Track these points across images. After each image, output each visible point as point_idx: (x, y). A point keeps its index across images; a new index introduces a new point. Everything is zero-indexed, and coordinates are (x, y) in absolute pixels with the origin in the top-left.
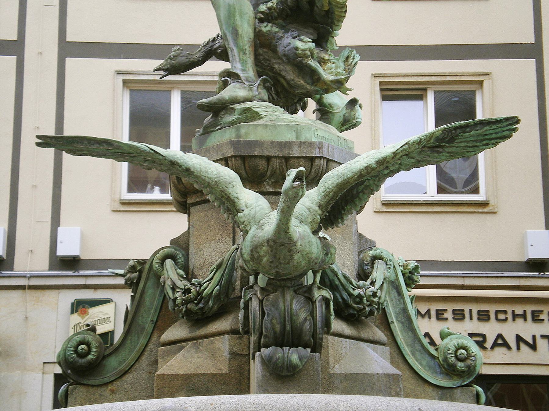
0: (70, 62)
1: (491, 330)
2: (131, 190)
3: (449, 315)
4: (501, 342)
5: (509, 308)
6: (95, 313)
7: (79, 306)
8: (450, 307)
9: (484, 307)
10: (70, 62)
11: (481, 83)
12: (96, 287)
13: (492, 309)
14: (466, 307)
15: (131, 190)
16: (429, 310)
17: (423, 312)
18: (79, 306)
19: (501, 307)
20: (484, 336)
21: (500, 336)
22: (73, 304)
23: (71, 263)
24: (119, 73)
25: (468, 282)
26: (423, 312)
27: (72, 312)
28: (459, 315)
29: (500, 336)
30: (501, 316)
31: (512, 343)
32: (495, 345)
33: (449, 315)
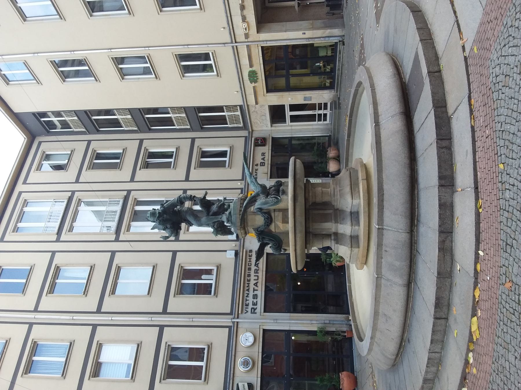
3: (249, 278)
5: (248, 263)
8: (247, 278)
9: (247, 269)
13: (247, 267)
14: (247, 273)
17: (247, 285)
19: (247, 264)
25: (240, 272)
28: (249, 275)
32: (257, 267)
33: (249, 278)
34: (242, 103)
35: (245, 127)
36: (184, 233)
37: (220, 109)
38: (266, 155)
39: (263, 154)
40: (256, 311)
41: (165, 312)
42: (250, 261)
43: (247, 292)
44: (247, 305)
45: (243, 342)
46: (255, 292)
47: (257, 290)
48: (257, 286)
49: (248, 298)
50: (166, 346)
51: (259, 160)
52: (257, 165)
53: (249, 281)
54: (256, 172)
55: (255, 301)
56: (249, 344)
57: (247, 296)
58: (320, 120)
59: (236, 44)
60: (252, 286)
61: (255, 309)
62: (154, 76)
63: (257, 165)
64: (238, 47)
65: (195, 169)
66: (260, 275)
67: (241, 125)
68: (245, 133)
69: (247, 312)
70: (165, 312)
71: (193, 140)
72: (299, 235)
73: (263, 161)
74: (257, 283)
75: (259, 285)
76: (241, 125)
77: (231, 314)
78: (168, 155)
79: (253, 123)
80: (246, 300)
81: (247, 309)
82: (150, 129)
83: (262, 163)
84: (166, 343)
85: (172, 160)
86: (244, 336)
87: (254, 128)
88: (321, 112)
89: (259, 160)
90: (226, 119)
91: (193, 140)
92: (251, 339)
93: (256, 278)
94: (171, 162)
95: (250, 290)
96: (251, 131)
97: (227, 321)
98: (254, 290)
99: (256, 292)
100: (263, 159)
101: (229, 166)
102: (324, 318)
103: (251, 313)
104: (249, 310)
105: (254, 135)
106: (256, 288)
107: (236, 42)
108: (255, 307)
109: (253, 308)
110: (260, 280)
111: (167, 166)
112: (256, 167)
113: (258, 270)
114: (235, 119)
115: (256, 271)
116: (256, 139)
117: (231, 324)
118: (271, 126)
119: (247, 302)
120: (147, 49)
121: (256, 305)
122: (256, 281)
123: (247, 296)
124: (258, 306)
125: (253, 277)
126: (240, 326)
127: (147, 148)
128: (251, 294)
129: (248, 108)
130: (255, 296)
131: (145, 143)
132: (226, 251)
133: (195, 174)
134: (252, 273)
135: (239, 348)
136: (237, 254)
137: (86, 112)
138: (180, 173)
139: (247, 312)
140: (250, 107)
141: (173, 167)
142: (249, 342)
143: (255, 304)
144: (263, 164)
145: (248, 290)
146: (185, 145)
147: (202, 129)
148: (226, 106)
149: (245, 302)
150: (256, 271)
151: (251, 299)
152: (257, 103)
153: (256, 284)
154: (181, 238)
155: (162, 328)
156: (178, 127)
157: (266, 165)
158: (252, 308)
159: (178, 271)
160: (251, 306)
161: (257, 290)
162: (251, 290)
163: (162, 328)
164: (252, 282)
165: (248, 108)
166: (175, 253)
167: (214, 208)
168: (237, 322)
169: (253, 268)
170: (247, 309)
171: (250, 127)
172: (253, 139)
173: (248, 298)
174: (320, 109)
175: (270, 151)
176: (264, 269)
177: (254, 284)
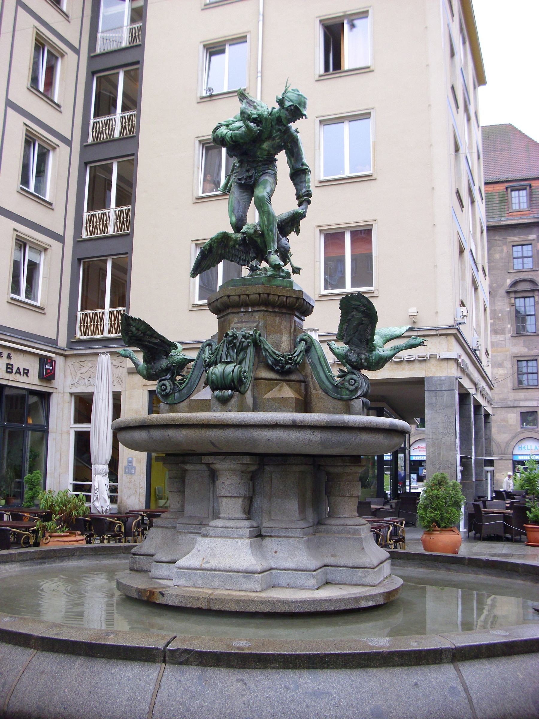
35: (73, 343)
58: (76, 488)
62: (201, 194)
67: (78, 336)
68: (63, 342)
72: (317, 436)
76: (78, 336)
79: (83, 359)
82: (86, 164)
87: (70, 361)
90: (97, 308)
91: (60, 239)
96: (67, 353)
105: (58, 357)
116: (52, 362)
118: (71, 394)
127: (58, 149)
131: (63, 148)
137: (138, 63)
146: (53, 220)
147: (78, 260)
171: (75, 352)
172: (53, 355)
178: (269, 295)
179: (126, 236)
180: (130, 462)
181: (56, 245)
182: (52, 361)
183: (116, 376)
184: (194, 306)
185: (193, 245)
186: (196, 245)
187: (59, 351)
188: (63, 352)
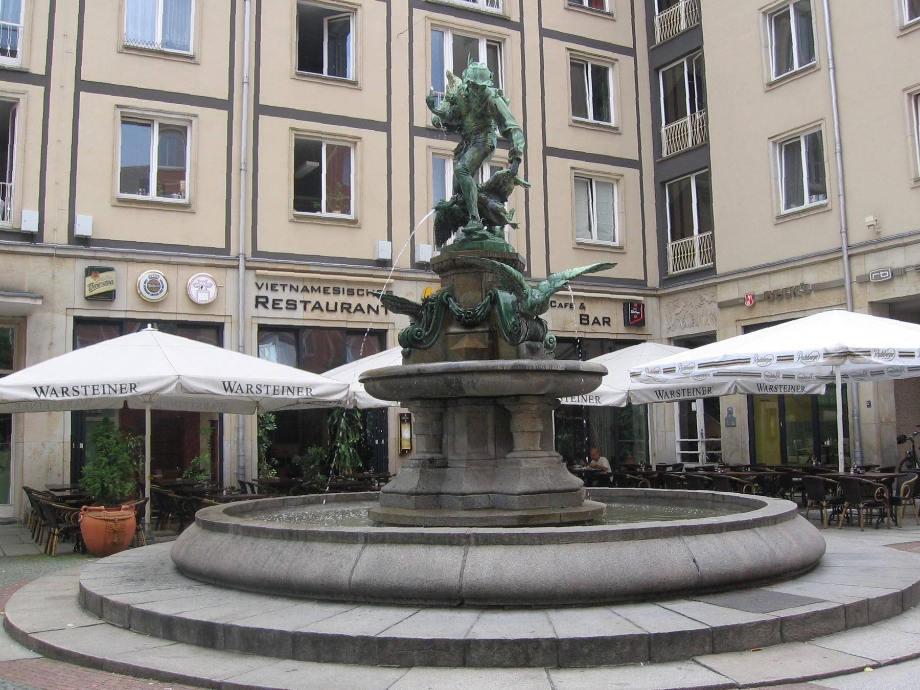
0: (83, 95)
1: (354, 301)
2: (122, 191)
3: (331, 291)
4: (359, 308)
6: (103, 276)
7: (90, 272)
10: (83, 95)
11: (355, 143)
12: (101, 259)
15: (122, 191)
16: (319, 288)
17: (316, 288)
18: (90, 272)
20: (350, 305)
21: (359, 305)
22: (87, 270)
23: (84, 241)
24: (118, 106)
25: (344, 271)
26: (316, 288)
27: (87, 275)
28: (337, 291)
29: (359, 305)
30: (360, 293)
31: (366, 310)
32: (356, 310)
34: (720, 269)
35: (667, 280)
36: (429, 147)
37: (707, 223)
38: (606, 328)
39: (607, 321)
40: (260, 306)
41: (260, 110)
42: (368, 293)
43: (300, 289)
44: (273, 288)
45: (196, 281)
46: (302, 305)
47: (305, 309)
48: (314, 308)
49: (287, 289)
50: (188, 115)
51: (594, 311)
52: (582, 307)
53: (326, 291)
54: (566, 306)
55: (283, 305)
56: (193, 291)
57: (291, 287)
58: (683, 446)
59: (845, 258)
60: (313, 298)
61: (264, 305)
62: (773, 78)
63: (582, 307)
64: (840, 263)
65: (572, 168)
66: (339, 315)
67: (670, 271)
68: (653, 280)
69: (260, 288)
70: (260, 110)
71: (636, 164)
73: (591, 321)
74: (320, 308)
75: (317, 314)
77: (256, 253)
78: (601, 109)
79: (677, 297)
80: (284, 286)
81: (264, 287)
82: (657, 70)
83: (588, 319)
84: (196, 116)
85: (591, 118)
86: (210, 281)
87: (665, 301)
88: (701, 449)
89: (594, 311)
90: (683, 237)
91: (636, 164)
92: (202, 298)
93: (332, 307)
94: (587, 117)
95: (305, 293)
96: (659, 293)
97: (241, 245)
98: (305, 303)
99: (300, 306)
100: (596, 321)
101: (579, 244)
102: (248, 454)
103: (257, 297)
104: (263, 292)
106: (309, 307)
107: (850, 256)
108: (270, 305)
109: (267, 301)
110: (328, 316)
111: (578, 107)
112: (576, 306)
113: (348, 310)
114: (685, 255)
115: (346, 307)
116: (640, 306)
117: (233, 253)
119: (280, 288)
120: (831, 65)
121: (274, 308)
122: (324, 306)
123: (291, 287)
124: (271, 313)
125: (332, 299)
126: (231, 273)
127: (617, 64)
128: (298, 297)
129: (709, 286)
130: (292, 305)
132: (390, 238)
133: (560, 168)
134: (342, 298)
135: (184, 272)
136: (384, 264)
138: (563, 134)
139: (260, 288)
140: (712, 290)
141: (575, 121)
142: (197, 292)
143: (275, 303)
144: (584, 320)
145: (305, 289)
146: (624, 147)
147: (660, 185)
148: (713, 236)
149: (279, 282)
150: (346, 307)
151: (285, 295)
152: (722, 306)
153: (317, 306)
154: (419, 141)
155: (226, 105)
156: (663, 130)
157: (583, 328)
158: (267, 298)
159: (345, 136)
160: (272, 296)
161: (305, 309)
162: (307, 297)
163: (226, 105)
164: (323, 299)
165: (709, 286)
166: (385, 127)
167: (493, 203)
168: (237, 267)
169: (354, 301)
170: (264, 287)
172: (641, 298)
173: (287, 289)
174: (709, 446)
175: (614, 337)
176: (350, 326)
177: (318, 303)
178: (454, 260)
179: (703, 147)
180: (730, 412)
181: (631, 174)
182: (639, 306)
183: (709, 313)
184: (780, 217)
185: (771, 144)
186: (775, 143)
187: (649, 292)
188: (654, 293)
